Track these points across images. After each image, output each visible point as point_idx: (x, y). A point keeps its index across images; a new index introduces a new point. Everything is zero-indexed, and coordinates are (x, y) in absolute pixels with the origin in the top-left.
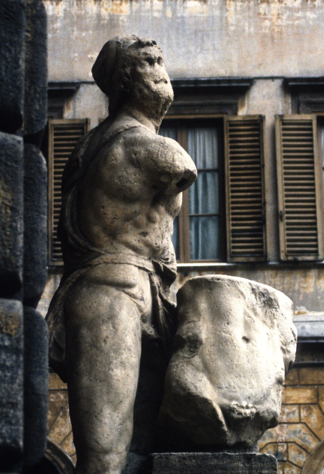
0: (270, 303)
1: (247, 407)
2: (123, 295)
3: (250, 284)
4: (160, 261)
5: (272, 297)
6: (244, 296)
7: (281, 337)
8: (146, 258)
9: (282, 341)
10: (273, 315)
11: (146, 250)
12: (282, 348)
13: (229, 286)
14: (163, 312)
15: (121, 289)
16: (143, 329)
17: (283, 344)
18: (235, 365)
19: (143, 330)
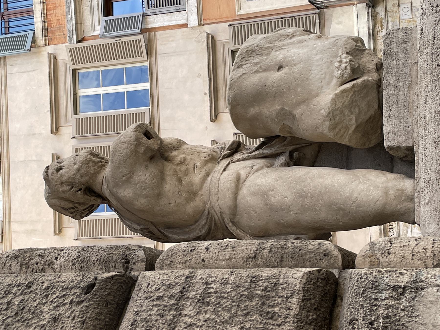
0: (250, 52)
1: (341, 62)
2: (247, 183)
6: (243, 74)
7: (281, 40)
11: (210, 165)
13: (234, 89)
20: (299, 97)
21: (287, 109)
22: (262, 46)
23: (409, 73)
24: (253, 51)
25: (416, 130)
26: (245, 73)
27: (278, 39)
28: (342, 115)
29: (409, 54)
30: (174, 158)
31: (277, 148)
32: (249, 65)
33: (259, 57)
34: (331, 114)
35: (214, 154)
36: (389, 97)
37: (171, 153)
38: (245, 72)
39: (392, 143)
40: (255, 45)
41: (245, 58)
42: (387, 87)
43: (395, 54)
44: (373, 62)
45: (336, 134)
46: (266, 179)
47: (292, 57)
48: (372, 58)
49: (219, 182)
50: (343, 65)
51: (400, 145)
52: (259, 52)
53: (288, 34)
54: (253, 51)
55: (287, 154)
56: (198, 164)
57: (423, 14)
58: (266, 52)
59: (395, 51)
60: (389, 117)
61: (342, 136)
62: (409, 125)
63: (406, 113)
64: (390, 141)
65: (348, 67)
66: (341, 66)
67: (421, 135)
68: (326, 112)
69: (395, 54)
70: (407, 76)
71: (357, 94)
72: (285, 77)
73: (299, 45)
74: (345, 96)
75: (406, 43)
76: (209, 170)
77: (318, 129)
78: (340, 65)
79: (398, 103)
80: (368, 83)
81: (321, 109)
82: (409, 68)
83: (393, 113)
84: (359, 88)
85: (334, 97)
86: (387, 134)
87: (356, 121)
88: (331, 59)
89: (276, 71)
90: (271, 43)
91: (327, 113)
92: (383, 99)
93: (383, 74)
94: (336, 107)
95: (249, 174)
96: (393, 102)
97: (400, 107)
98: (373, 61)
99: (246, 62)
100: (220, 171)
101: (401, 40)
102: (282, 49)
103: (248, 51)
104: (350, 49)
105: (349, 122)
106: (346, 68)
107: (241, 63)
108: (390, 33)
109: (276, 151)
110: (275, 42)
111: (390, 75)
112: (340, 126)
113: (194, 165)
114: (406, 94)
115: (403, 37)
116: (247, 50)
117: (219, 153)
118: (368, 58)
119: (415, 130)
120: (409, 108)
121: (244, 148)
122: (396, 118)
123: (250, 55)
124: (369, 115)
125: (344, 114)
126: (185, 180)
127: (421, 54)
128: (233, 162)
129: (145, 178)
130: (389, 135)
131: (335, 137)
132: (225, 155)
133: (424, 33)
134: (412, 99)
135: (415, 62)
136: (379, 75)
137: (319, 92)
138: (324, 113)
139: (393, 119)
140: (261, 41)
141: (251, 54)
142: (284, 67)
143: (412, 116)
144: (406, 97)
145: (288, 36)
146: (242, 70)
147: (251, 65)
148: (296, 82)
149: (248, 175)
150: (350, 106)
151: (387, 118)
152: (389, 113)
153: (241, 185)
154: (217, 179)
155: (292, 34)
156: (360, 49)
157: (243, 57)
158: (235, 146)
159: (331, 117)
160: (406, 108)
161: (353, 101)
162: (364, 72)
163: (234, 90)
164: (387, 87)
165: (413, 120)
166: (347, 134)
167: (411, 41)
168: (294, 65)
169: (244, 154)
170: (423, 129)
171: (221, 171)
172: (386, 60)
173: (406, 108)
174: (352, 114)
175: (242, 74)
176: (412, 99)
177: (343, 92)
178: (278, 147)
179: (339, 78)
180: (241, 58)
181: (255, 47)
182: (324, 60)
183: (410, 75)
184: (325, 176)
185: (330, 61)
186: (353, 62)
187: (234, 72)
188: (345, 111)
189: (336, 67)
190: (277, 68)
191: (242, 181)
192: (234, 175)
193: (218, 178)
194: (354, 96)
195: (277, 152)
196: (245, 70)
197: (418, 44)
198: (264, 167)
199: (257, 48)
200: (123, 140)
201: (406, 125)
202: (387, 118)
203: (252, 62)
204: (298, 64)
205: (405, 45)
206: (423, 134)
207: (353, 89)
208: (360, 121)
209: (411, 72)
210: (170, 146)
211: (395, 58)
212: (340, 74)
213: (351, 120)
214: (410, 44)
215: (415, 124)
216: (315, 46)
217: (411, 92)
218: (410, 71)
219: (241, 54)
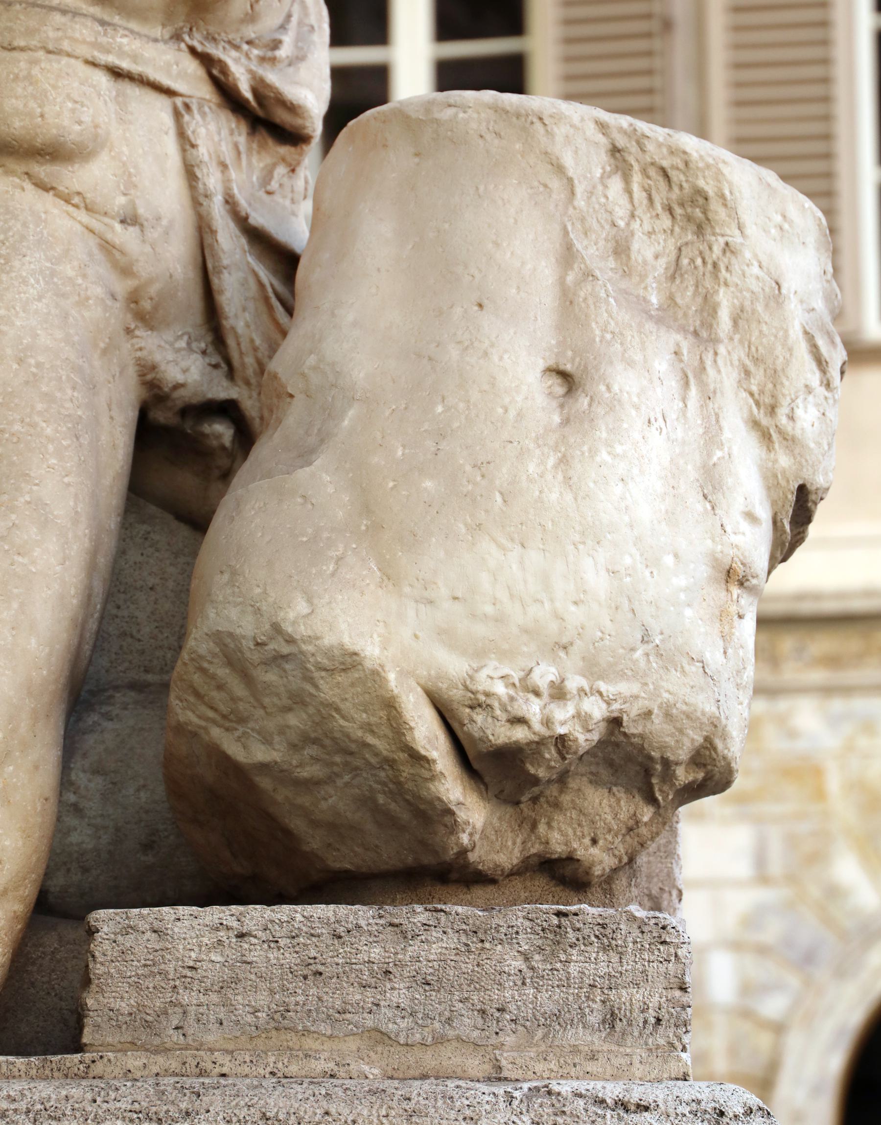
0: (698, 213)
1: (559, 693)
3: (602, 127)
4: (234, 53)
6: (570, 180)
7: (747, 373)
8: (158, 31)
9: (754, 389)
10: (710, 267)
12: (755, 424)
13: (497, 134)
14: (244, 283)
15: (20, 167)
16: (139, 354)
17: (757, 404)
18: (497, 494)
19: (139, 359)
20: (391, 484)
21: (346, 422)
22: (723, 273)
23: (451, 1033)
24: (700, 230)
25: (160, 1062)
26: (573, 193)
27: (756, 361)
28: (286, 702)
29: (545, 1036)
31: (252, 341)
32: (621, 212)
33: (662, 262)
34: (286, 650)
36: (340, 937)
38: (579, 189)
39: (107, 945)
40: (736, 239)
41: (662, 183)
42: (392, 925)
43: (558, 965)
44: (587, 841)
45: (205, 665)
46: (40, 298)
47: (609, 444)
48: (609, 837)
49: (41, 54)
50: (533, 709)
51: (93, 987)
52: (692, 261)
54: (700, 230)
55: (222, 391)
57: (722, 1114)
58: (686, 297)
59: (573, 969)
60: (241, 936)
61: (198, 695)
62: (190, 1031)
63: (249, 1019)
64: (120, 938)
65: (520, 734)
66: (532, 697)
67: (113, 1095)
68: (294, 623)
69: (558, 965)
70: (437, 1025)
71: (382, 774)
72: (506, 411)
73: (692, 472)
74: (373, 720)
75: (604, 1021)
77: (226, 577)
78: (537, 693)
79: (305, 977)
80: (442, 830)
81: (310, 601)
82: (476, 1033)
83: (256, 955)
84: (410, 785)
85: (368, 664)
86: (156, 924)
87: (264, 768)
88: (578, 642)
89: (551, 362)
91: (290, 630)
92: (332, 907)
93: (459, 909)
94: (316, 675)
95: (87, 209)
96: (313, 953)
97: (284, 989)
98: (594, 841)
99: (639, 194)
100: (108, 52)
101: (624, 996)
102: (687, 384)
103: (701, 201)
104: (641, 736)
105: (259, 733)
106: (519, 721)
107: (636, 167)
108: (664, 943)
109: (237, 337)
110: (741, 342)
111: (452, 941)
112: (239, 689)
114: (348, 1016)
115: (636, 1007)
116: (711, 193)
117: (250, 32)
118: (609, 818)
119: (160, 1059)
120: (274, 1032)
121: (274, 166)
122: (232, 968)
123: (678, 211)
124: (297, 824)
125: (290, 709)
127: (516, 1103)
130: (148, 934)
131: (192, 660)
133: (620, 1119)
134: (316, 1045)
135: (504, 1063)
136: (516, 873)
137: (407, 590)
138: (291, 615)
139: (227, 951)
140: (755, 270)
141: (689, 218)
142: (562, 406)
143: (231, 1047)
144: (329, 1017)
145: (772, 410)
146: (598, 173)
147: (622, 224)
148: (468, 468)
149: (76, 200)
150: (327, 742)
151: (235, 924)
152: (260, 934)
153: (20, 168)
154: (58, 40)
155: (780, 432)
156: (654, 781)
157: (673, 174)
158: (282, 116)
159: (272, 646)
160: (277, 1016)
161: (351, 753)
162: (518, 803)
163: (489, 137)
164: (392, 925)
165: (211, 1050)
166: (208, 719)
167: (614, 1048)
168: (564, 461)
169: (224, 166)
170: (136, 1106)
171: (111, 59)
172: (527, 923)
173: (277, 1016)
174: (294, 747)
175: (571, 173)
176: (316, 1045)
177: (391, 705)
178: (258, 342)
179: (466, 688)
180: (665, 164)
181: (722, 240)
182: (573, 608)
183: (440, 1040)
184: (15, 605)
185: (564, 640)
186: (559, 752)
187: (591, 129)
188: (305, 716)
189: (531, 670)
190: (568, 368)
191: (42, 170)
192: (77, 128)
193: (66, 45)
194: (373, 760)
195: (231, 342)
196: (591, 193)
197: (575, 1084)
198: (131, 283)
199: (717, 250)
201: (191, 1017)
202: (235, 924)
203: (636, 225)
204: (567, 479)
205: (594, 1019)
206: (111, 1106)
207: (402, 756)
208: (265, 783)
209: (454, 1044)
211: (532, 969)
212: (487, 694)
213: (267, 741)
214: (597, 1041)
215: (189, 1060)
216: (669, 560)
217: (352, 1044)
218: (458, 1039)
219: (687, 164)
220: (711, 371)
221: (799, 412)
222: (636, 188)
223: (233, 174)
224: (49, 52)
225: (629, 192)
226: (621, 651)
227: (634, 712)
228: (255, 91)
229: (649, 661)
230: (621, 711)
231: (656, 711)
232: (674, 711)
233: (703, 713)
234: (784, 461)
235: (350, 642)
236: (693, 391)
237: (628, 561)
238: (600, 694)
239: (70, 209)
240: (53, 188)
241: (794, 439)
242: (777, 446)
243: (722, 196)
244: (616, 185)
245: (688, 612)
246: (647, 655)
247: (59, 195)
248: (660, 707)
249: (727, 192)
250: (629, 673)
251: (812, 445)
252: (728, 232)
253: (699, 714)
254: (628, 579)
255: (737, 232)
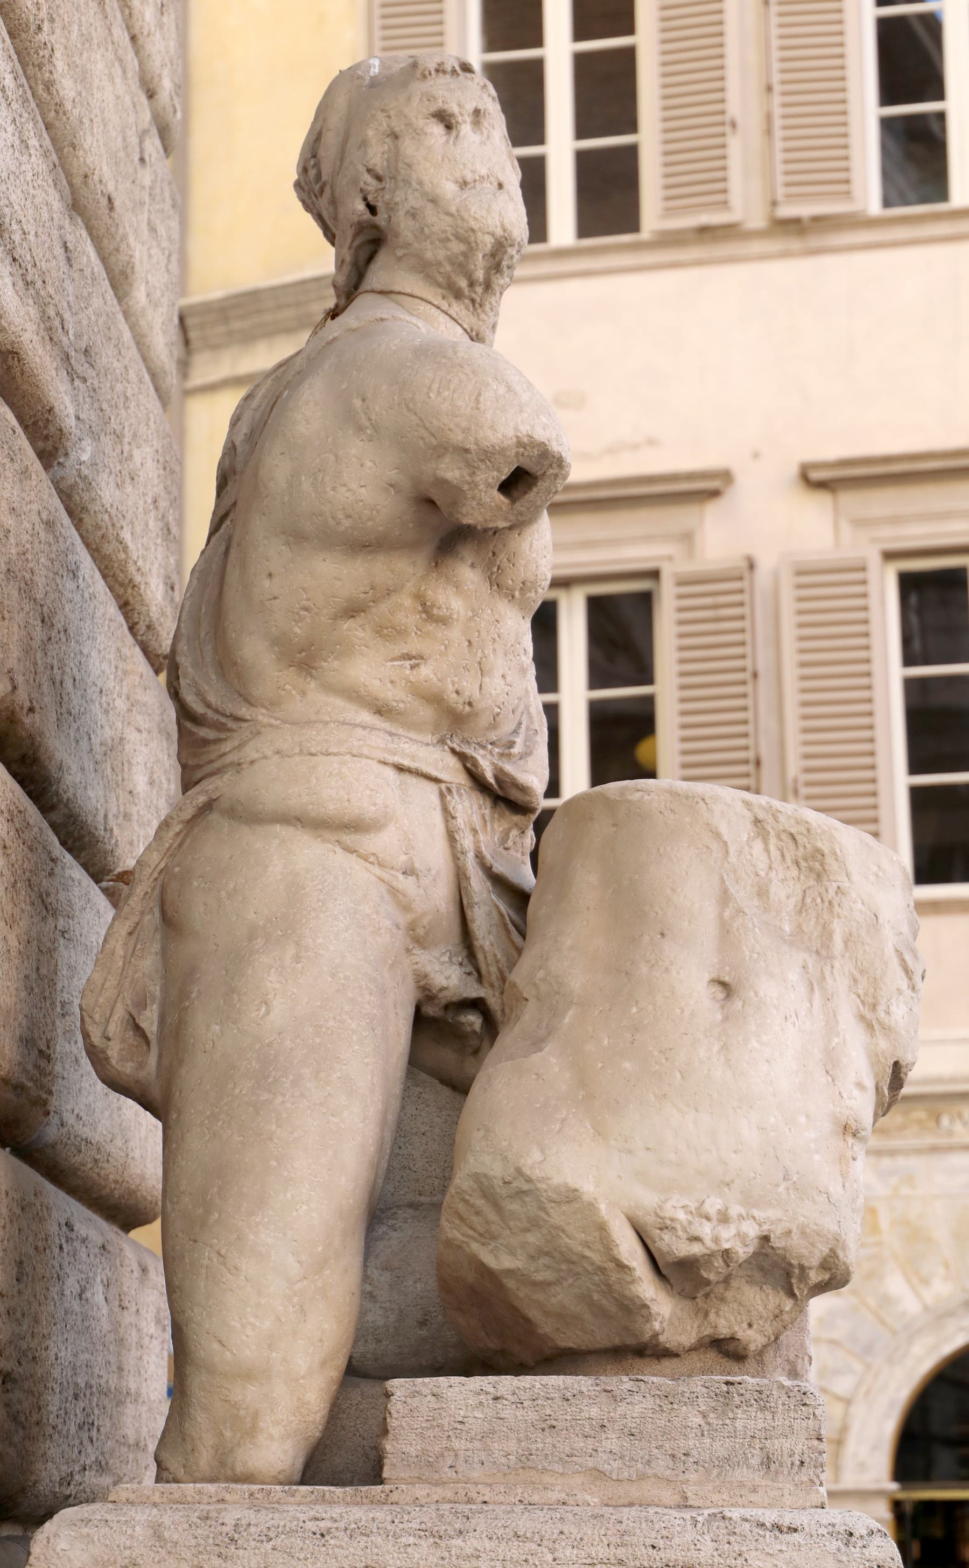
0: (817, 865)
1: (724, 1218)
2: (339, 858)
3: (748, 804)
4: (482, 752)
5: (825, 848)
6: (725, 843)
7: (855, 981)
8: (429, 738)
9: (861, 992)
10: (826, 904)
11: (426, 713)
12: (862, 1018)
14: (489, 914)
15: (334, 837)
16: (415, 967)
17: (863, 1003)
18: (677, 1072)
19: (416, 970)
20: (600, 1065)
21: (567, 1020)
22: (836, 909)
23: (650, 1472)
24: (819, 877)
25: (438, 1493)
26: (727, 852)
27: (862, 972)
28: (526, 1225)
29: (719, 1474)
30: (448, 580)
31: (495, 955)
32: (762, 866)
33: (792, 901)
34: (525, 1187)
35: (484, 720)
36: (568, 1400)
37: (473, 566)
38: (732, 849)
39: (399, 1406)
40: (846, 884)
41: (791, 845)
42: (605, 1391)
43: (728, 1421)
44: (745, 1325)
45: (467, 1197)
46: (347, 930)
48: (761, 1323)
49: (348, 757)
50: (706, 1230)
51: (390, 1435)
52: (814, 900)
53: (881, 1009)
54: (819, 877)
55: (473, 991)
56: (425, 671)
57: (851, 1534)
58: (810, 926)
59: (739, 1424)
60: (496, 1399)
61: (462, 1219)
62: (460, 1469)
63: (503, 1460)
64: (409, 1400)
65: (696, 1249)
66: (704, 1221)
67: (406, 1517)
68: (532, 1168)
69: (728, 1421)
70: (640, 1466)
71: (597, 1278)
72: (683, 1011)
74: (589, 1238)
75: (762, 1464)
76: (400, 713)
77: (481, 1133)
78: (708, 1219)
79: (543, 1430)
80: (640, 1319)
81: (542, 1151)
82: (668, 1472)
83: (507, 1413)
84: (616, 1287)
85: (585, 1198)
86: (435, 1390)
87: (510, 1272)
89: (714, 975)
90: (846, 943)
91: (528, 1173)
92: (562, 1377)
93: (655, 1379)
94: (548, 1205)
95: (379, 865)
96: (548, 1412)
97: (528, 1438)
98: (750, 1325)
99: (774, 853)
100: (395, 754)
101: (778, 1445)
102: (812, 989)
103: (819, 857)
104: (784, 1249)
105: (506, 1247)
106: (696, 1239)
107: (772, 833)
108: (805, 1405)
109: (484, 953)
110: (850, 958)
111: (649, 1403)
112: (492, 1216)
113: (422, 658)
114: (575, 1459)
115: (785, 1453)
116: (826, 852)
117: (493, 736)
118: (761, 1308)
119: (439, 1490)
120: (521, 1471)
121: (510, 830)
122: (490, 1422)
124: (534, 1314)
125: (528, 1230)
126: (355, 630)
127: (699, 1525)
128: (442, 796)
129: (354, 486)
130: (430, 1397)
131: (458, 1193)
132: (475, 763)
133: (776, 1538)
134: (551, 1480)
135: (689, 1494)
136: (693, 1349)
137: (613, 1142)
138: (530, 1162)
139: (486, 1410)
140: (859, 906)
141: (811, 869)
142: (723, 1007)
143: (490, 1481)
144: (561, 1459)
145: (874, 1007)
146: (745, 838)
147: (763, 874)
148: (656, 1053)
149: (372, 859)
150: (556, 1254)
151: (491, 1390)
152: (510, 1397)
155: (880, 1023)
156: (794, 1281)
157: (798, 837)
158: (515, 795)
159: (515, 1184)
160: (523, 1459)
161: (573, 1263)
162: (694, 1298)
163: (666, 813)
164: (605, 1391)
165: (476, 1484)
166: (469, 1236)
167: (770, 1483)
168: (725, 1047)
169: (474, 831)
170: (423, 1526)
171: (397, 759)
172: (705, 1390)
173: (523, 1459)
174: (532, 1258)
175: (726, 838)
176: (551, 1480)
177: (602, 1228)
178: (499, 956)
179: (657, 1215)
180: (793, 831)
181: (835, 885)
182: (733, 1155)
183: (642, 1477)
184: (330, 1153)
185: (728, 1179)
186: (725, 1262)
187: (740, 807)
188: (539, 1235)
189: (703, 1202)
190: (727, 979)
191: (348, 839)
192: (373, 808)
193: (365, 751)
194: (590, 1268)
195: (480, 956)
196: (740, 852)
197: (742, 1511)
198: (410, 917)
199: (832, 892)
200: (487, 396)
201: (461, 1458)
202: (491, 1390)
203: (773, 875)
204: (728, 1061)
205: (755, 1461)
206: (406, 1526)
207: (611, 1265)
208: (510, 1284)
209: (653, 1480)
210: (502, 557)
211: (709, 1424)
212: (672, 1220)
213: (512, 1253)
214: (757, 1478)
215: (460, 1491)
216: (802, 1119)
217: (578, 1479)
218: (656, 1476)
219: (808, 830)
220: (829, 980)
221: (893, 1009)
222: (772, 848)
223: (481, 837)
224: (354, 756)
225: (768, 851)
226: (769, 1186)
227: (778, 1232)
228: (496, 778)
229: (789, 1194)
230: (769, 1230)
231: (794, 1230)
232: (808, 1230)
233: (829, 1231)
234: (883, 1044)
235: (573, 1182)
236: (817, 995)
237: (773, 1120)
238: (754, 1218)
239: (368, 865)
240: (355, 851)
241: (889, 1028)
242: (877, 1033)
243: (835, 853)
244: (758, 845)
245: (817, 1157)
246: (788, 1189)
247: (360, 856)
248: (798, 1228)
249: (838, 851)
250: (775, 1202)
251: (903, 1032)
252: (840, 879)
253: (826, 1232)
254: (773, 1134)
255: (846, 879)
